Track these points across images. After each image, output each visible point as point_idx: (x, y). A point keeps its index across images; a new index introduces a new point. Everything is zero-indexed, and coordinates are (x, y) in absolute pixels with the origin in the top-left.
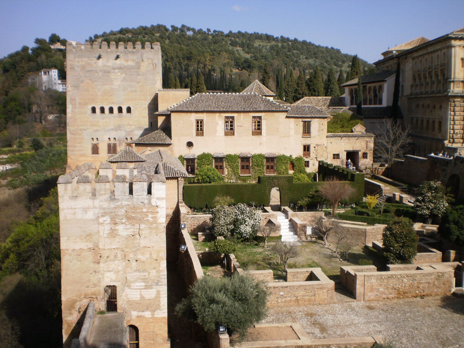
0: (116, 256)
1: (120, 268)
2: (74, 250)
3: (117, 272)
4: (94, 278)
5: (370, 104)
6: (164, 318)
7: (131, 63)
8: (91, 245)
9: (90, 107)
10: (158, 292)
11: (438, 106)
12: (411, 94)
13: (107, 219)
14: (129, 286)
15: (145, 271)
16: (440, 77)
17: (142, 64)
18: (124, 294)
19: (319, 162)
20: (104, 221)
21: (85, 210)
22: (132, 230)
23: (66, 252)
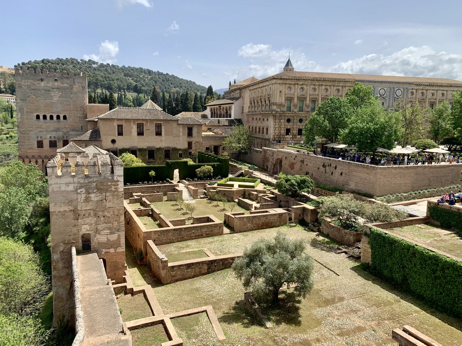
0: (89, 215)
1: (93, 222)
2: (59, 212)
3: (91, 225)
4: (75, 230)
5: (224, 117)
6: (123, 252)
7: (66, 85)
8: (72, 208)
9: (35, 115)
10: (119, 236)
11: (266, 120)
12: (249, 112)
13: (83, 190)
14: (99, 234)
15: (110, 222)
16: (267, 102)
17: (74, 86)
18: (96, 238)
19: (199, 152)
20: (81, 191)
21: (67, 184)
22: (101, 197)
23: (54, 213)
